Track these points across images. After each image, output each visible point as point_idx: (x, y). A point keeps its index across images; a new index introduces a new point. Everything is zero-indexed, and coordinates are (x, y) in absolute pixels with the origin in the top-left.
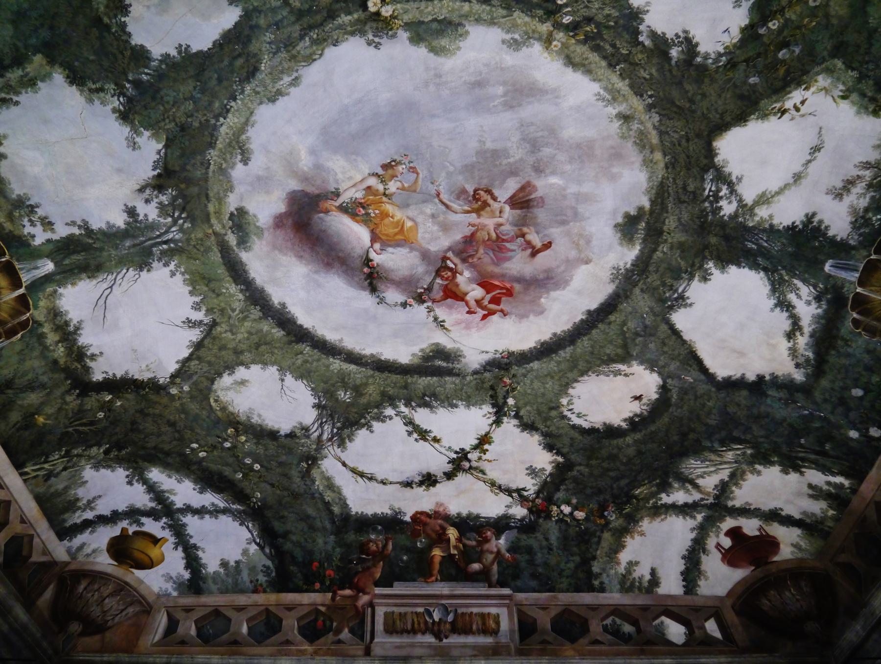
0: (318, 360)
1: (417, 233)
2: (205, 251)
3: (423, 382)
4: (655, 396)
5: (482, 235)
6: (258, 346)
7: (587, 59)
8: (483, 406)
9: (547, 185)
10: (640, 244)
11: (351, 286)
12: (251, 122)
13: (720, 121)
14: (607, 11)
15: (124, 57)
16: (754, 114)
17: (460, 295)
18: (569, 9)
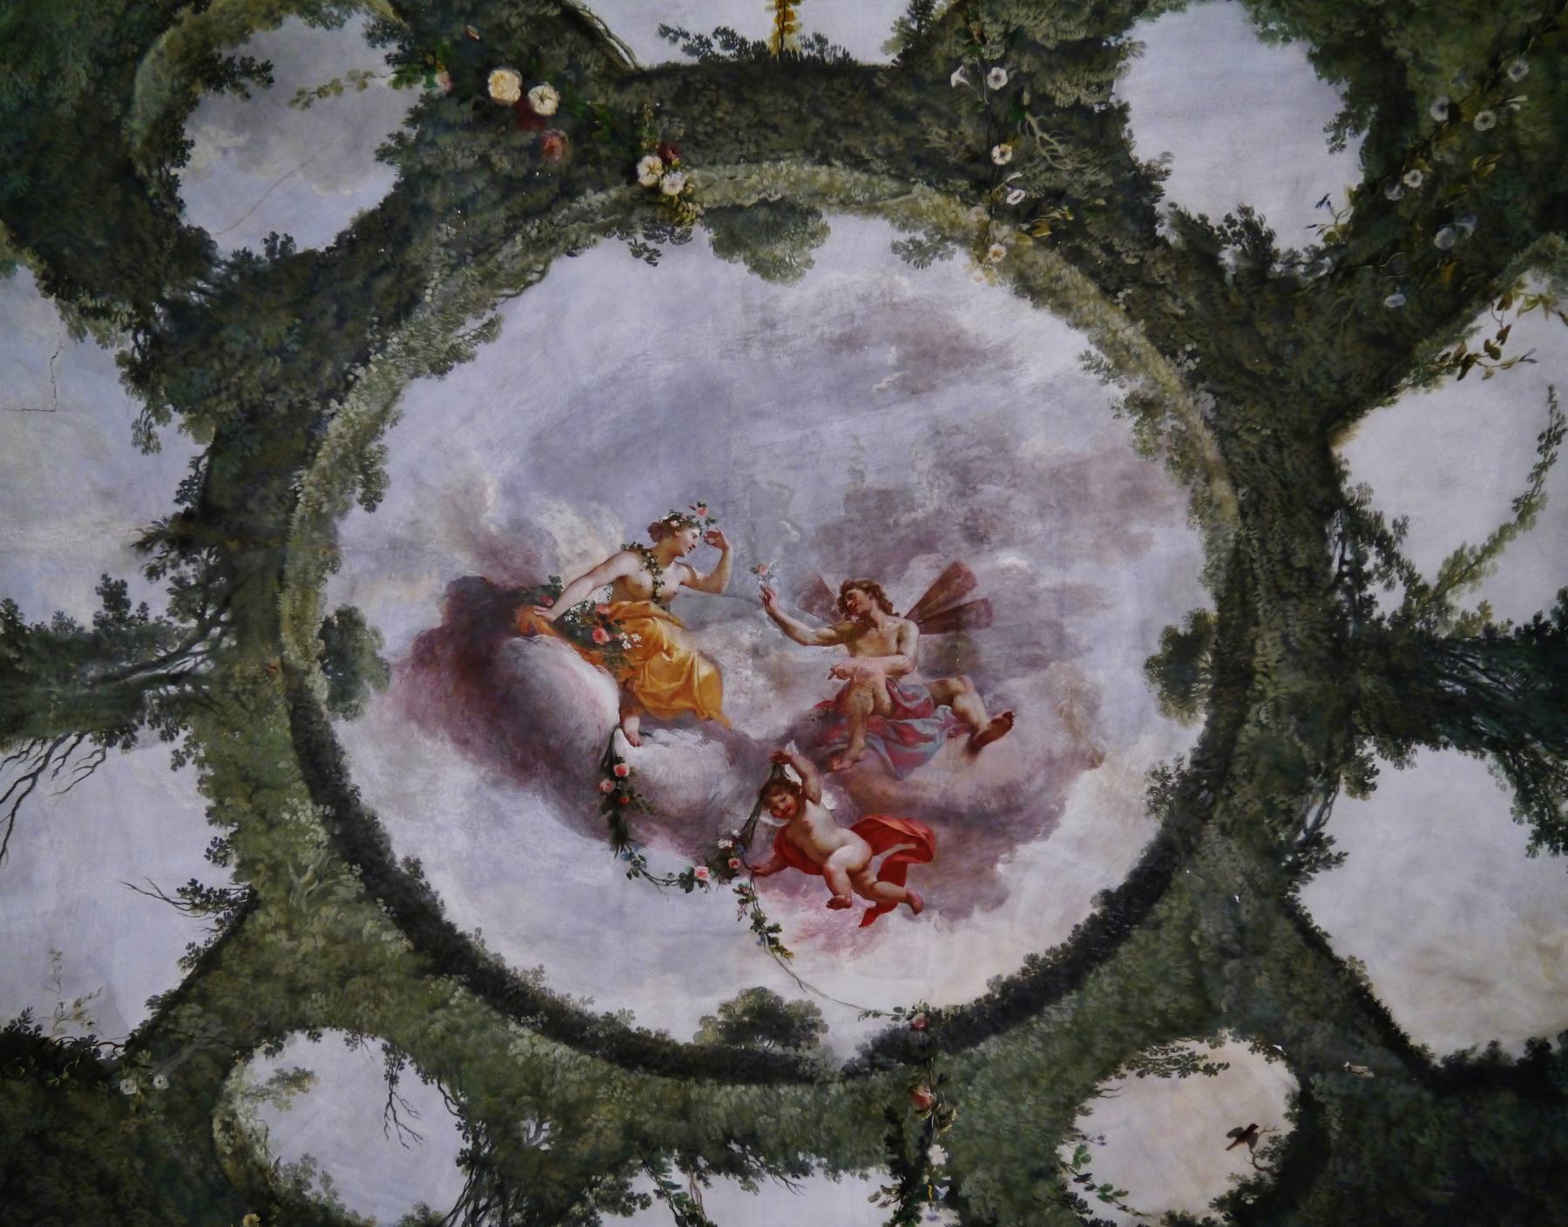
0: (483, 1027)
1: (721, 693)
2: (257, 710)
3: (727, 1098)
4: (1287, 1128)
5: (861, 700)
6: (345, 976)
7: (1059, 279)
8: (872, 1171)
9: (998, 569)
10: (1207, 707)
11: (573, 826)
12: (392, 415)
13: (1339, 398)
14: (1090, 177)
15: (162, 250)
16: (1406, 375)
17: (814, 857)
18: (1018, 175)
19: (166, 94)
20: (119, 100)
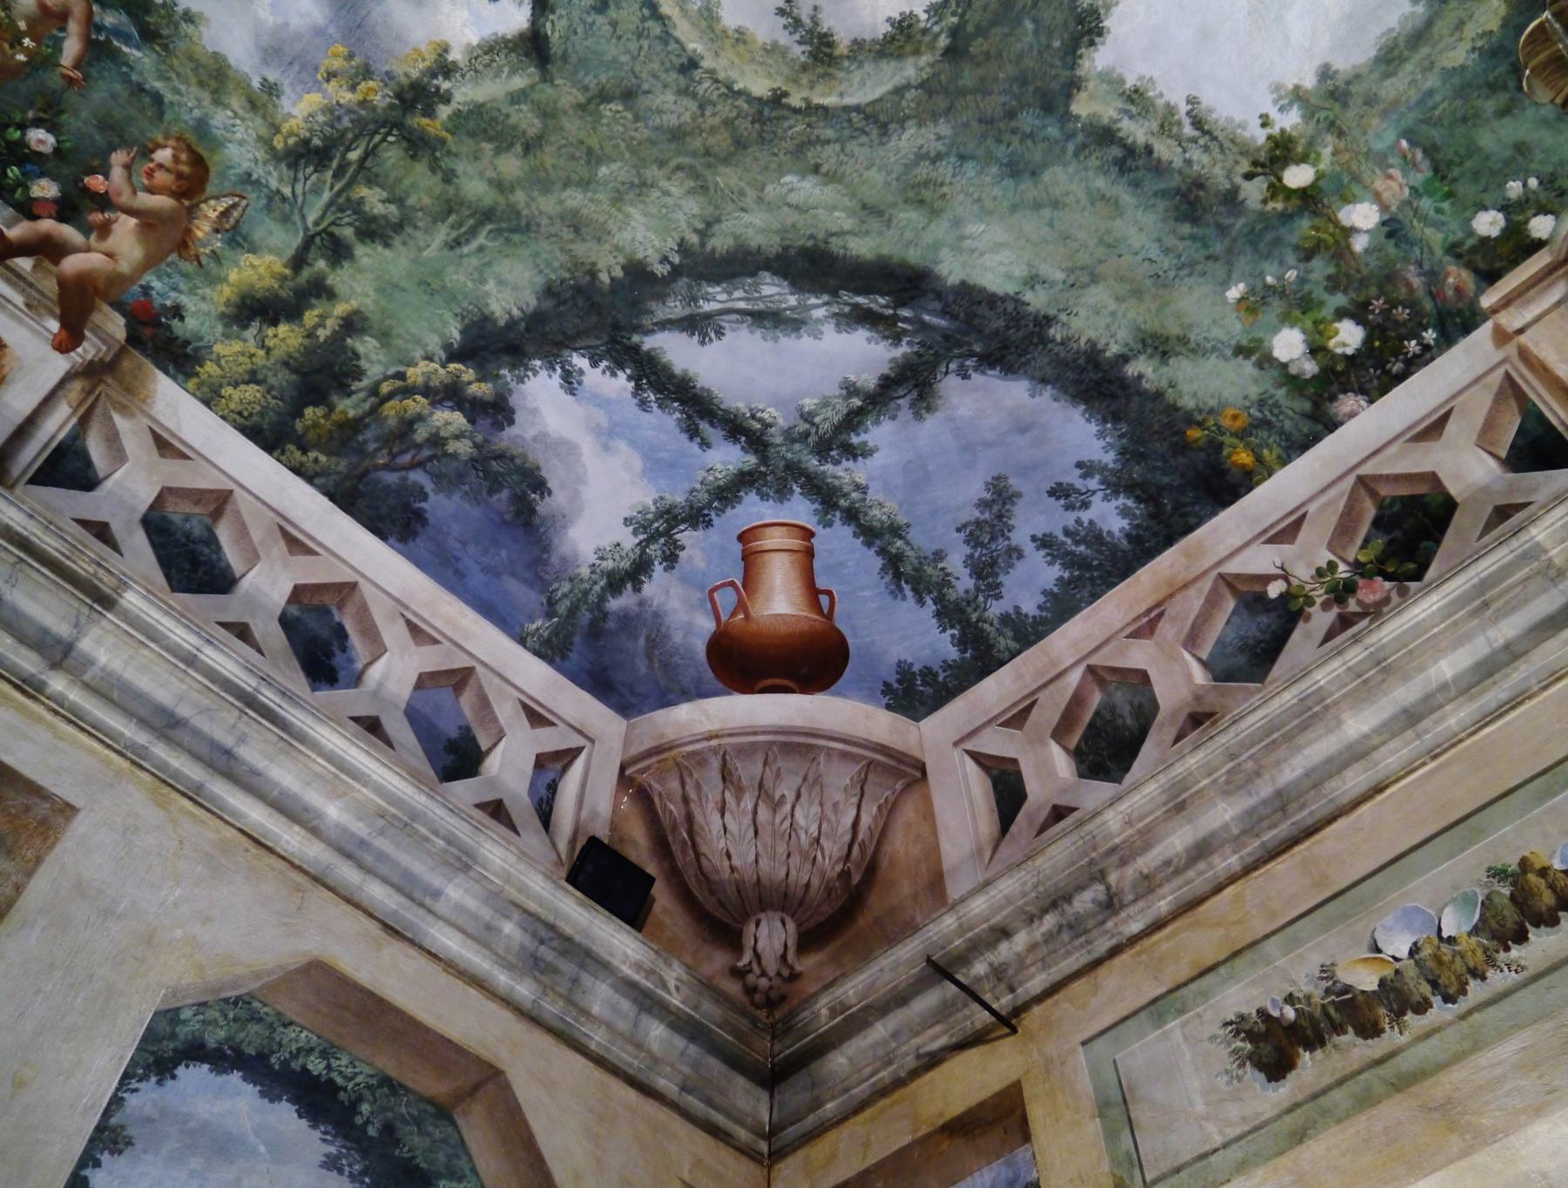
19: (868, 67)
20: (903, 97)
